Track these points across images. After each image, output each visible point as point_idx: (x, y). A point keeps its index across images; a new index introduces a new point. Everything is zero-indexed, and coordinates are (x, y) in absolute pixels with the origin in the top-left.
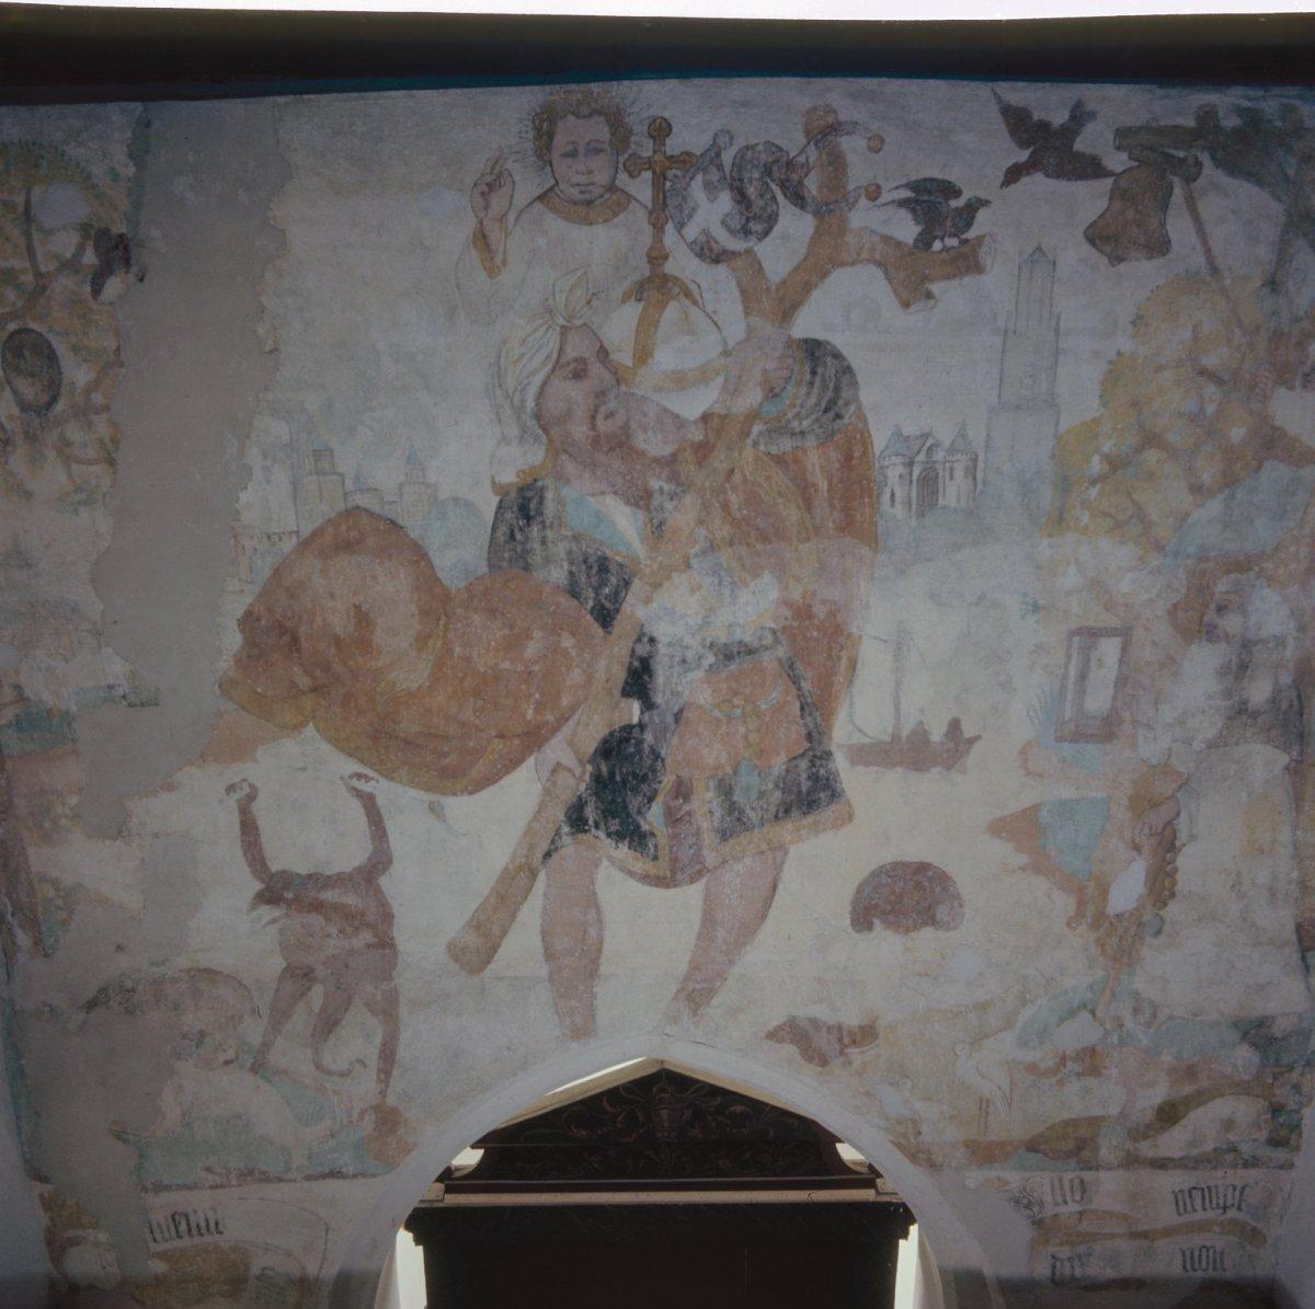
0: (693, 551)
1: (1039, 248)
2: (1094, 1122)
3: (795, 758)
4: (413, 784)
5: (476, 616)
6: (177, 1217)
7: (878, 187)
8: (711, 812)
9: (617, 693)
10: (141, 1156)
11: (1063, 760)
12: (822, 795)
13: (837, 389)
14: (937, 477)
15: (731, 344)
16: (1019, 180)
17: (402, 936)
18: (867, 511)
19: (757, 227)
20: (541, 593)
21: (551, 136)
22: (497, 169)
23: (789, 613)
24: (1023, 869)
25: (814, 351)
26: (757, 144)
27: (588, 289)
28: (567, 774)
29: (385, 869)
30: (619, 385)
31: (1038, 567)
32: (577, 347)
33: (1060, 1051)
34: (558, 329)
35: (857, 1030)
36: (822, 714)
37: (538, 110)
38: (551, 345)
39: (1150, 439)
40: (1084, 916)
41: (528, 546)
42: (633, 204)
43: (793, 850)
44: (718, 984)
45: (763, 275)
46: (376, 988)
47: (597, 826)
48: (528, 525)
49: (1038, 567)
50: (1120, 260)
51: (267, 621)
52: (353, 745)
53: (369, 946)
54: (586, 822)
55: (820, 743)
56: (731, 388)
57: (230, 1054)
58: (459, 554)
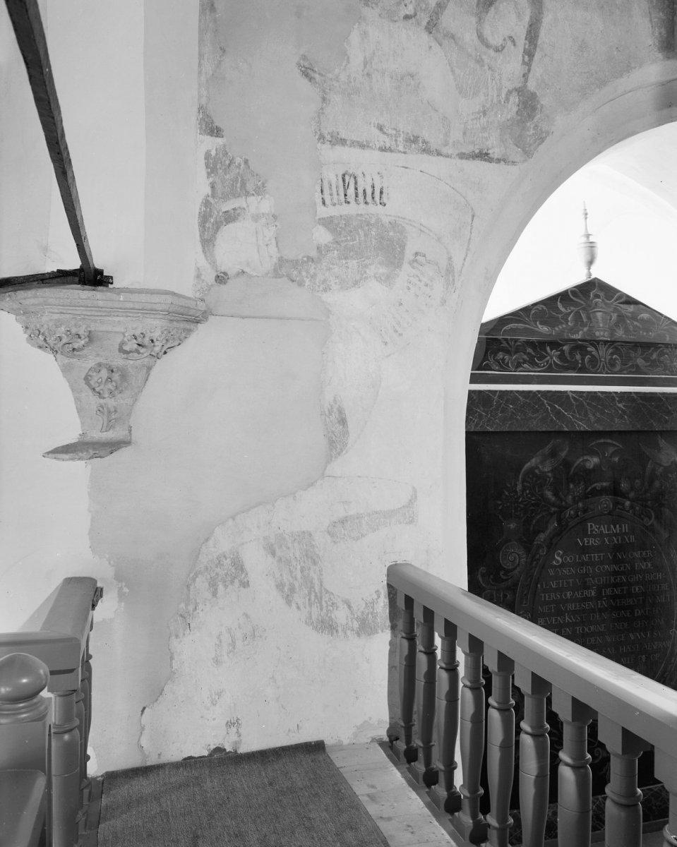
6: (347, 178)
10: (324, 99)
57: (410, 10)
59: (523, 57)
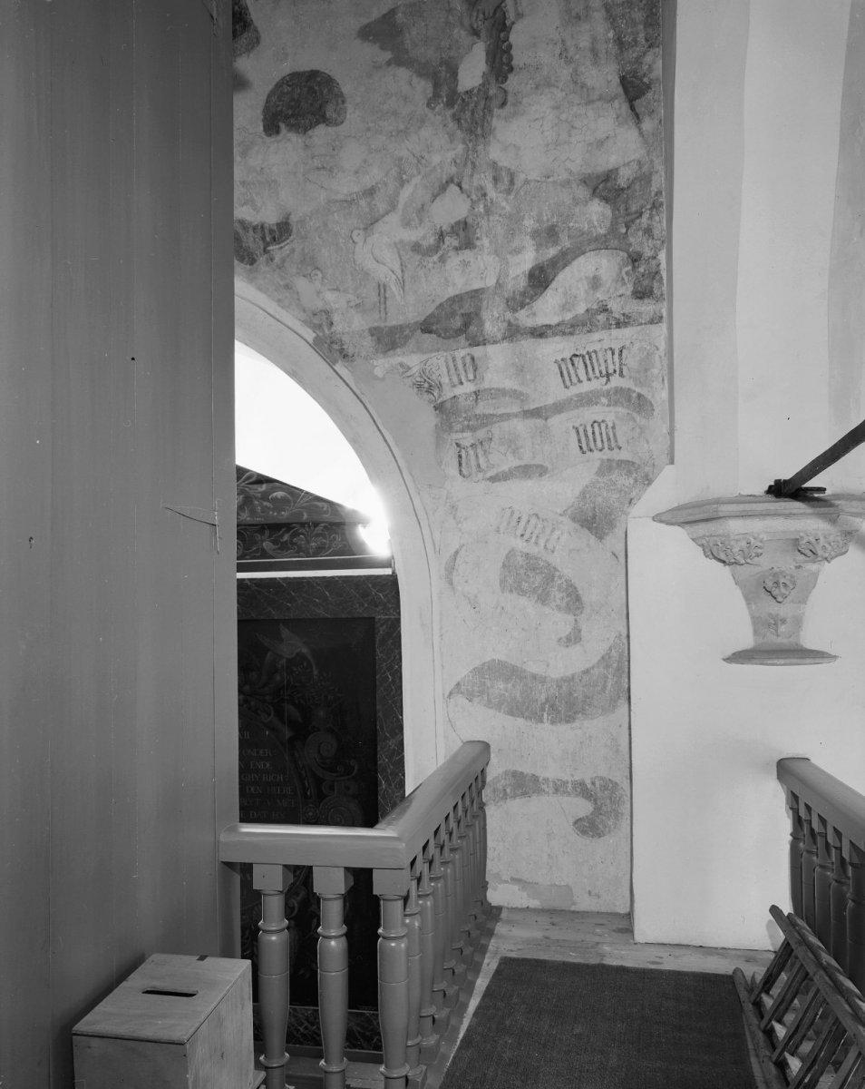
2: (476, 295)
24: (389, 63)
40: (439, 96)
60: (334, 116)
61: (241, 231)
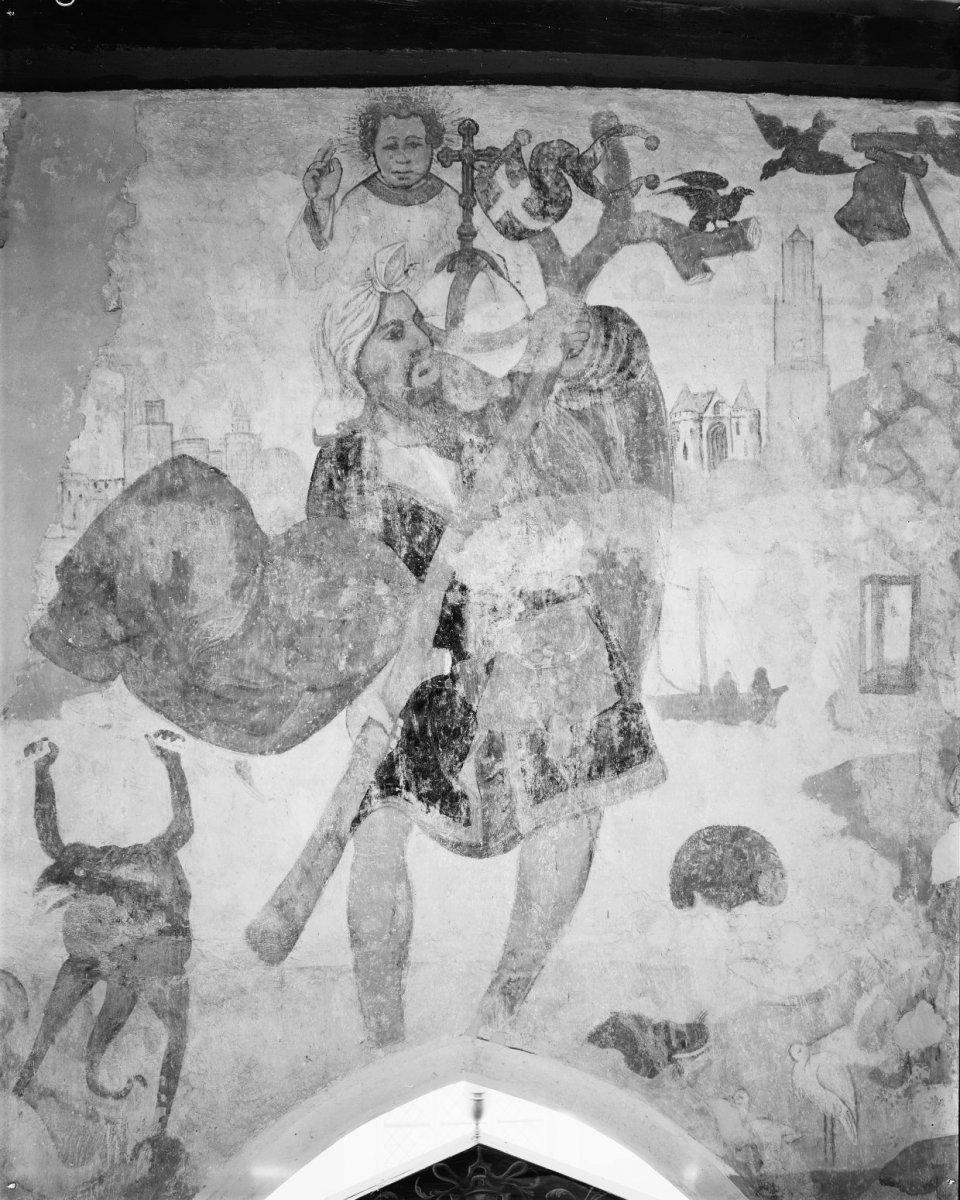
0: (501, 501)
1: (798, 230)
3: (605, 711)
4: (219, 743)
5: (292, 562)
7: (656, 177)
8: (523, 771)
9: (429, 643)
11: (870, 713)
12: (635, 752)
13: (630, 351)
14: (725, 432)
15: (533, 311)
16: (775, 174)
17: (197, 917)
18: (663, 463)
19: (552, 209)
20: (356, 541)
21: (375, 132)
22: (327, 158)
23: (594, 561)
24: (843, 833)
25: (607, 317)
26: (552, 142)
27: (405, 261)
28: (380, 729)
29: (185, 841)
30: (433, 345)
31: (825, 517)
32: (396, 311)
33: (904, 1051)
34: (378, 295)
35: (685, 1030)
36: (630, 664)
37: (364, 111)
38: (372, 309)
39: (913, 398)
40: (909, 886)
41: (346, 495)
42: (446, 189)
43: (608, 813)
44: (535, 974)
45: (560, 252)
46: (165, 983)
47: (408, 789)
48: (346, 475)
49: (825, 517)
50: (869, 240)
51: (86, 568)
52: (160, 700)
53: (161, 932)
54: (396, 783)
55: (630, 695)
56: (534, 349)
58: (279, 501)
59: (159, 1097)
60: (770, 892)
61: (636, 1030)
